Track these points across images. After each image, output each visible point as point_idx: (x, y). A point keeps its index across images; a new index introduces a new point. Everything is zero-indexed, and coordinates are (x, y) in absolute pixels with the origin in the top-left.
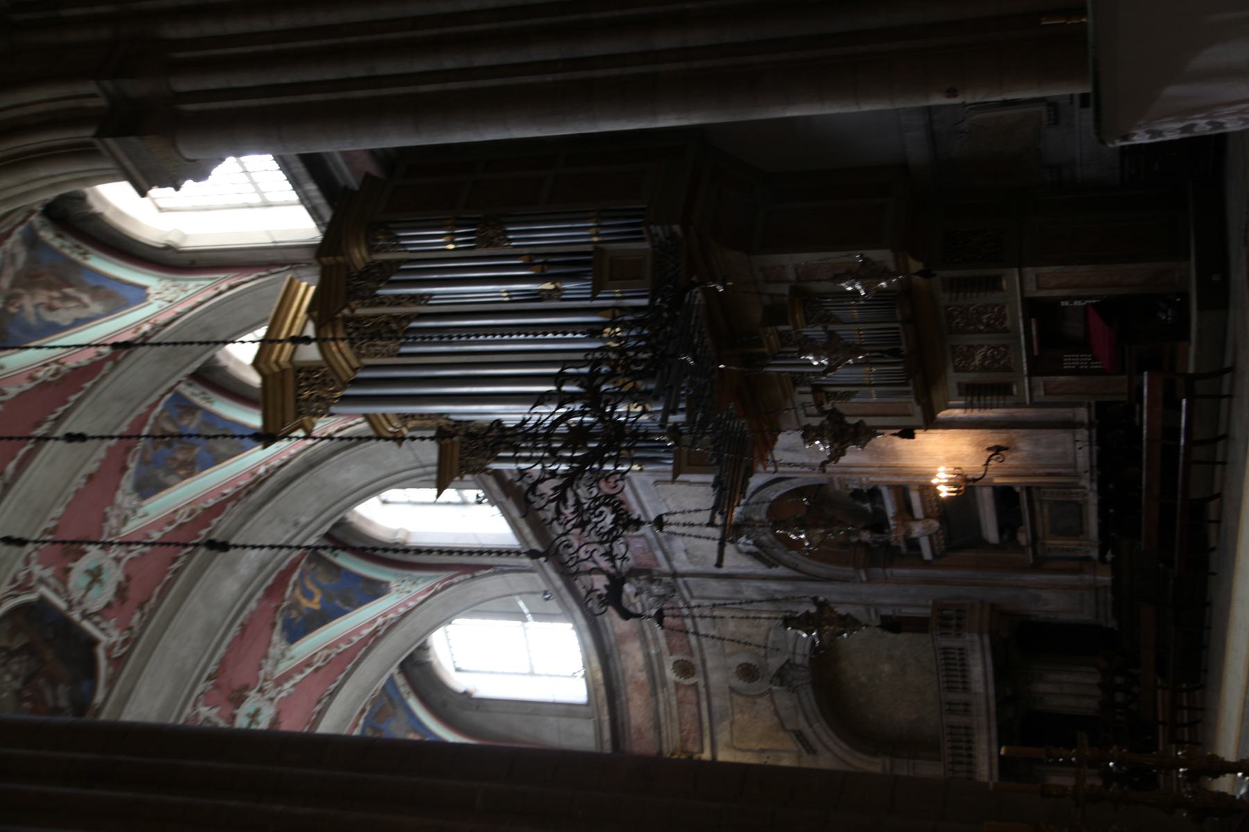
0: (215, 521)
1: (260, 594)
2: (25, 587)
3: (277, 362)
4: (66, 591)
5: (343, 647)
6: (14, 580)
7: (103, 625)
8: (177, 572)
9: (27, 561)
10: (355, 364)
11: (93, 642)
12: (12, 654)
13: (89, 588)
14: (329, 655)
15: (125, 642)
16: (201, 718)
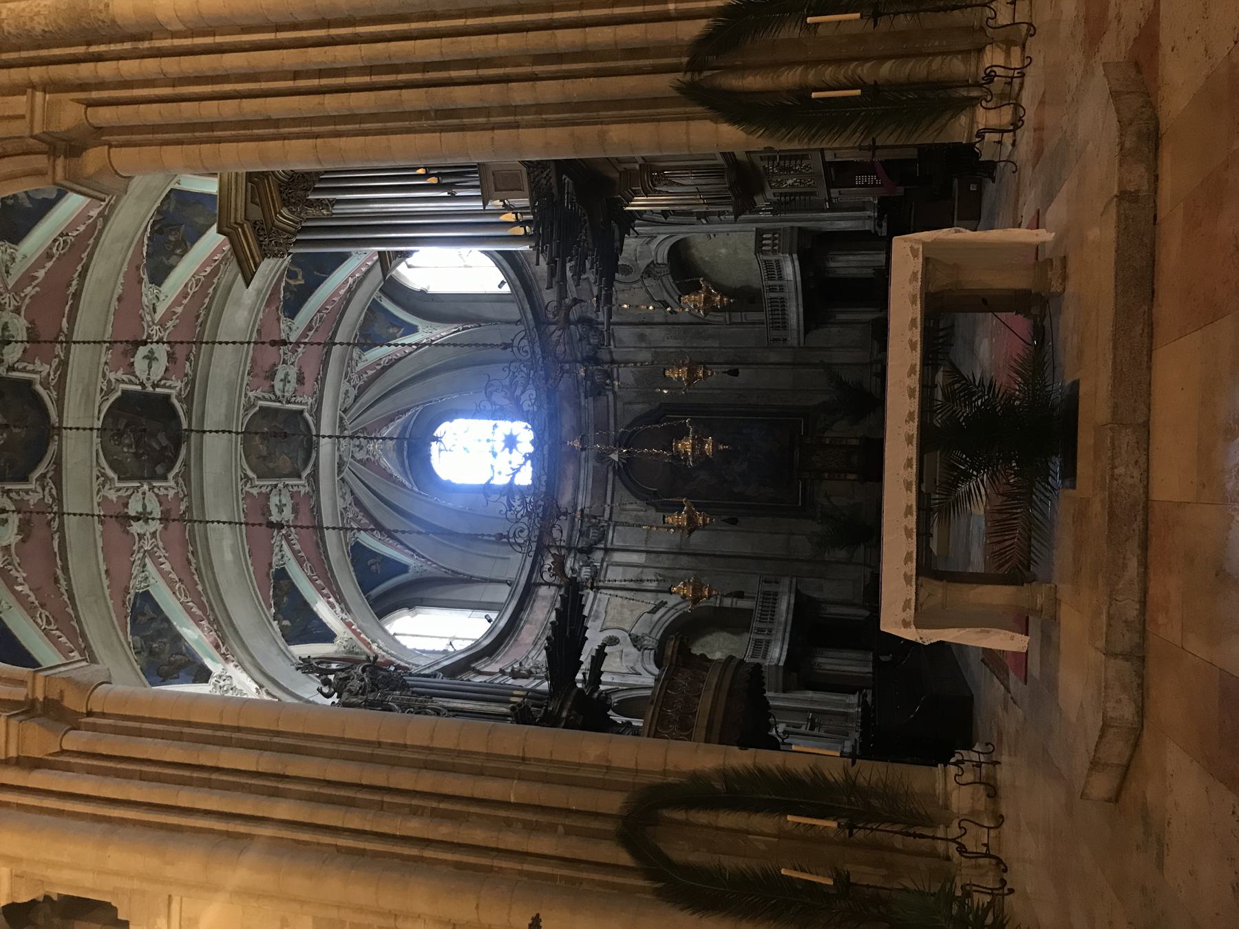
0: (215, 280)
1: (263, 307)
2: (111, 390)
3: (236, 223)
4: (136, 377)
5: (329, 307)
6: (102, 390)
7: (167, 384)
8: (203, 324)
9: (104, 376)
10: (297, 219)
11: (168, 397)
12: (120, 434)
13: (150, 367)
14: (321, 318)
15: (186, 384)
16: (252, 400)
